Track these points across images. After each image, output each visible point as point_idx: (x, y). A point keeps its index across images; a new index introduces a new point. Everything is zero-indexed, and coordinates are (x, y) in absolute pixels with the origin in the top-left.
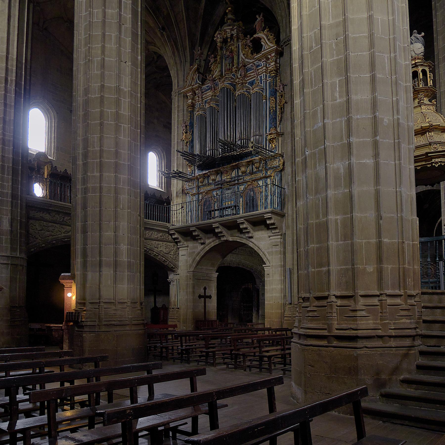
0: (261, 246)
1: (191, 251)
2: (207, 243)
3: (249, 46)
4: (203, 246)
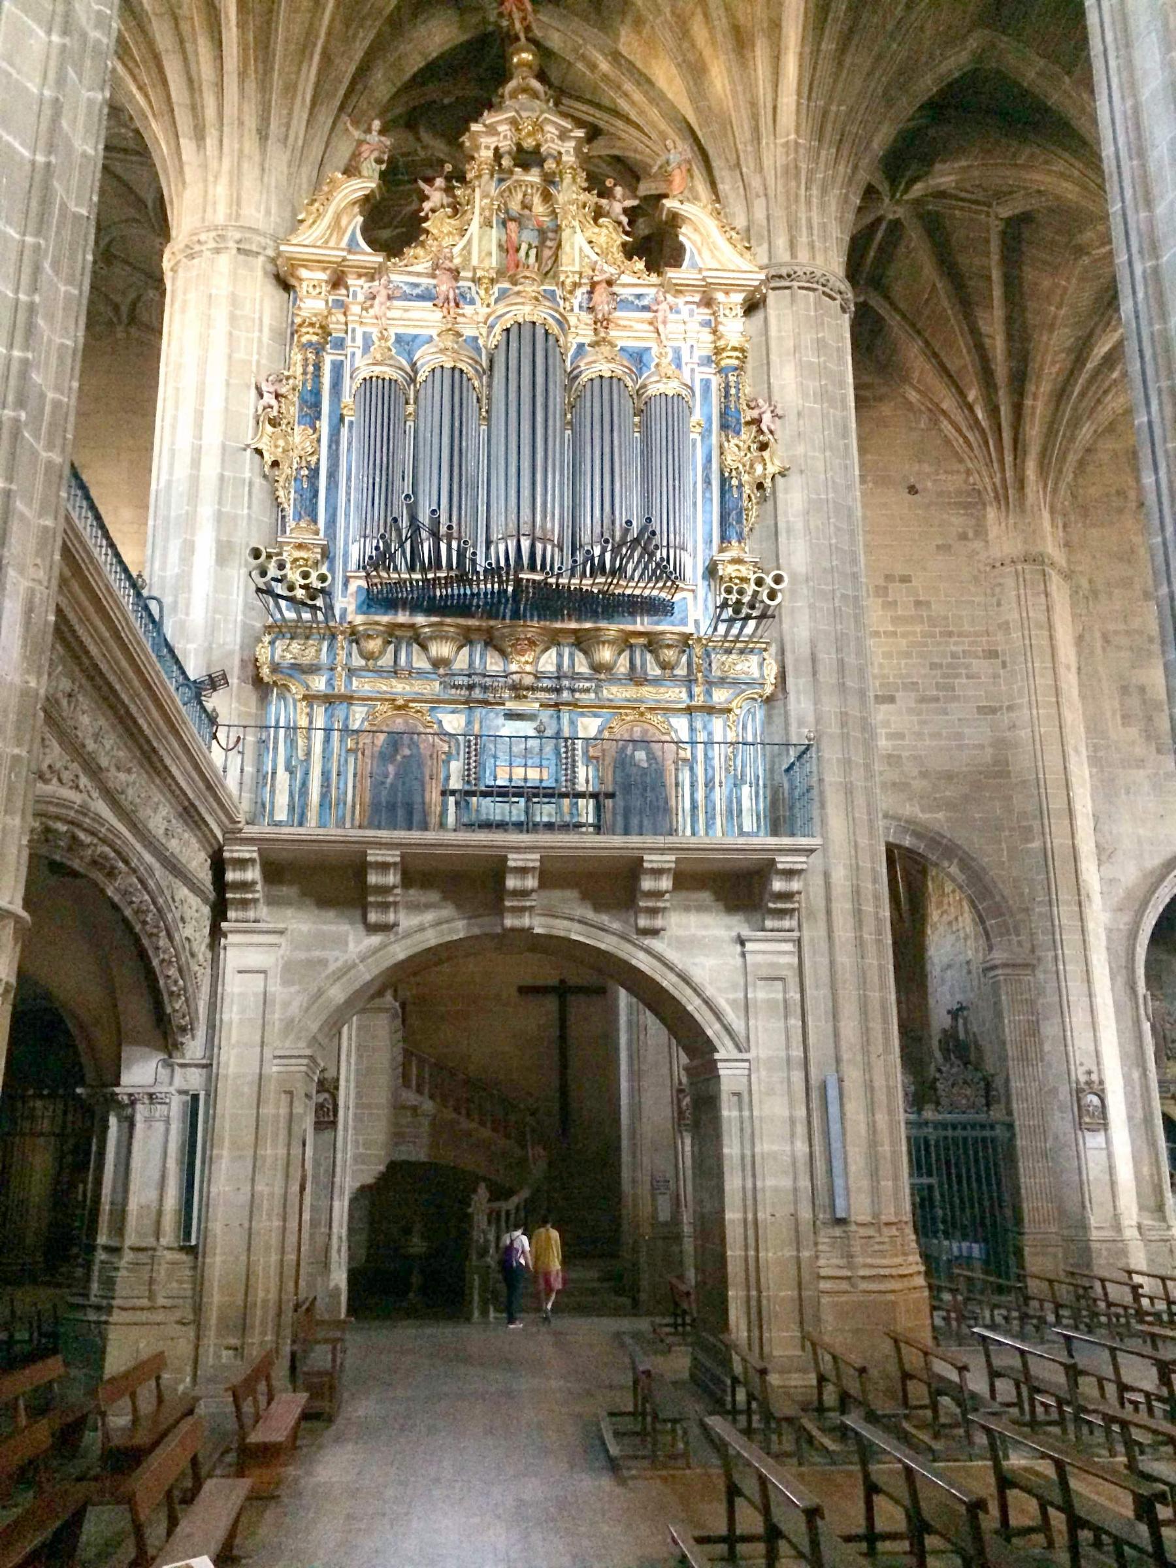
0: (699, 975)
1: (302, 955)
2: (400, 929)
3: (620, 223)
4: (376, 940)
